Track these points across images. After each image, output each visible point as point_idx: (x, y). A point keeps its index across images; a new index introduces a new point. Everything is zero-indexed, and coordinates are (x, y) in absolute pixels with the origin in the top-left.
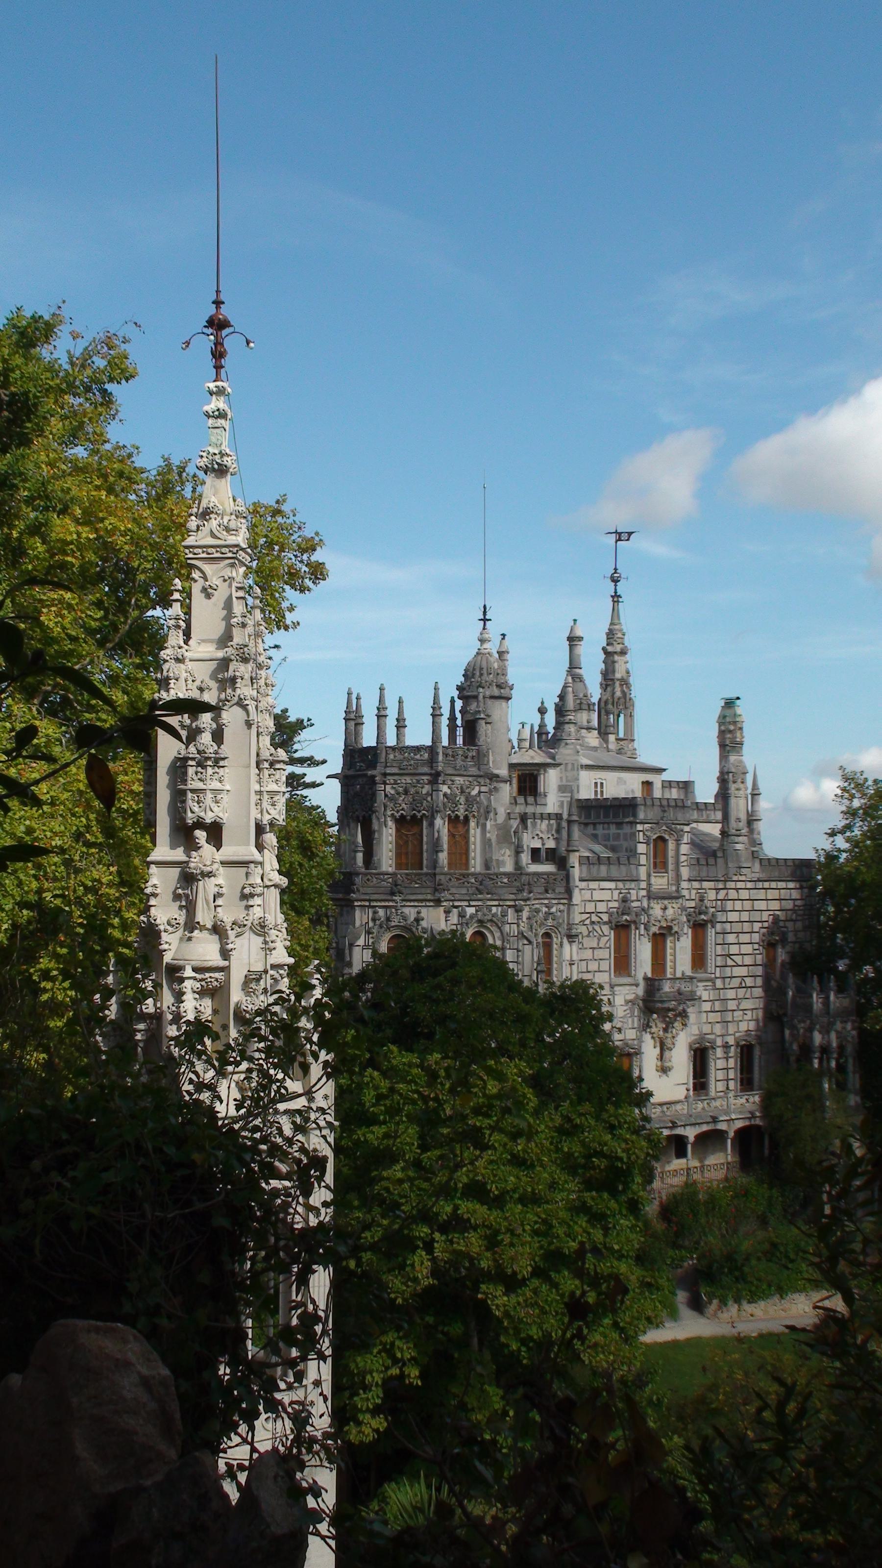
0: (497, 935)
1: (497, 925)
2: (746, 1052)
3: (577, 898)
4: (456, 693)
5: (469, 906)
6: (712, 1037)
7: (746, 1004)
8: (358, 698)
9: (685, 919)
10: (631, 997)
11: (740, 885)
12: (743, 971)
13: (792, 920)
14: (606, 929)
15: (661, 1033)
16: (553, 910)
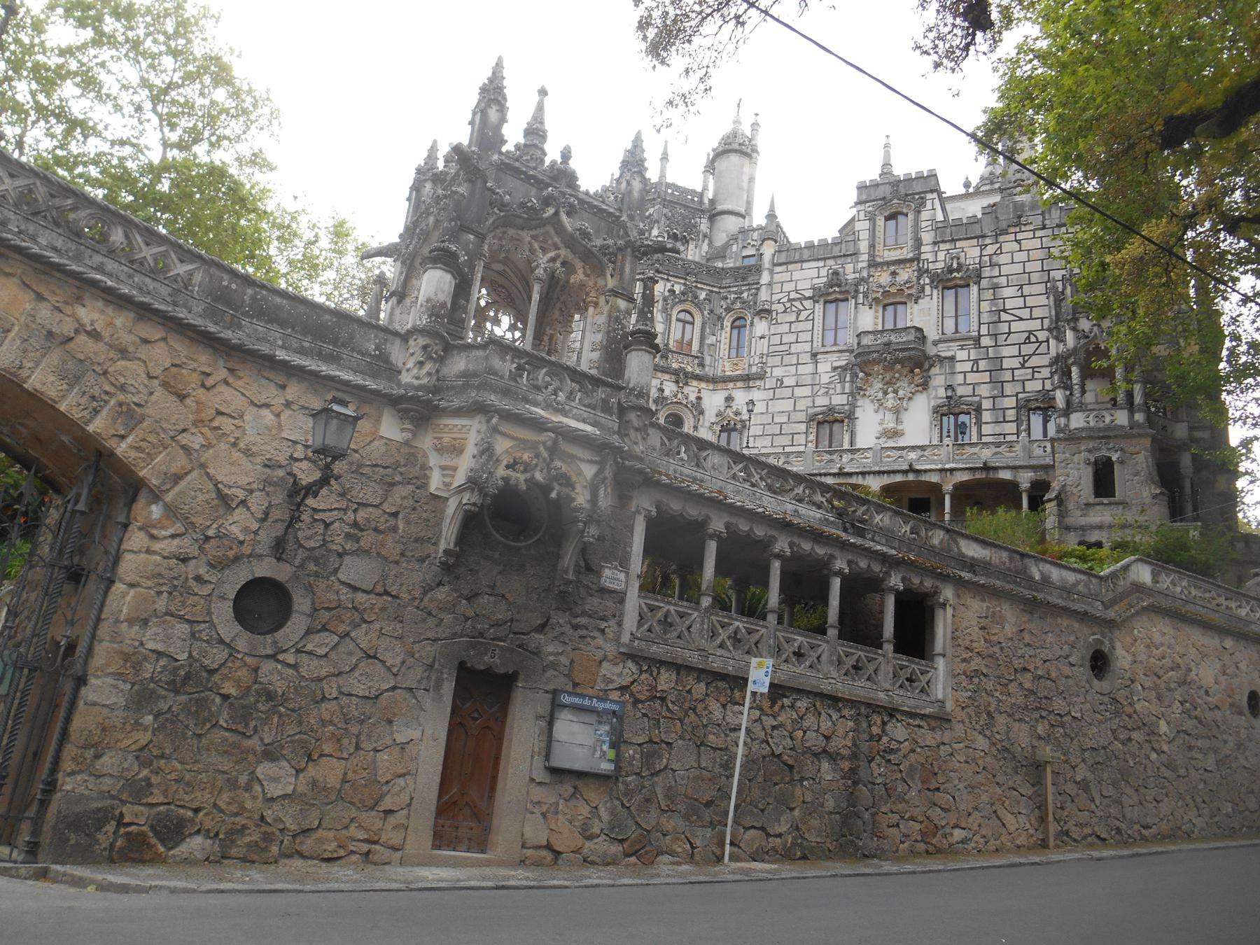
6: (977, 399)
9: (927, 281)
11: (1019, 236)
12: (1036, 325)
14: (808, 304)
15: (880, 395)
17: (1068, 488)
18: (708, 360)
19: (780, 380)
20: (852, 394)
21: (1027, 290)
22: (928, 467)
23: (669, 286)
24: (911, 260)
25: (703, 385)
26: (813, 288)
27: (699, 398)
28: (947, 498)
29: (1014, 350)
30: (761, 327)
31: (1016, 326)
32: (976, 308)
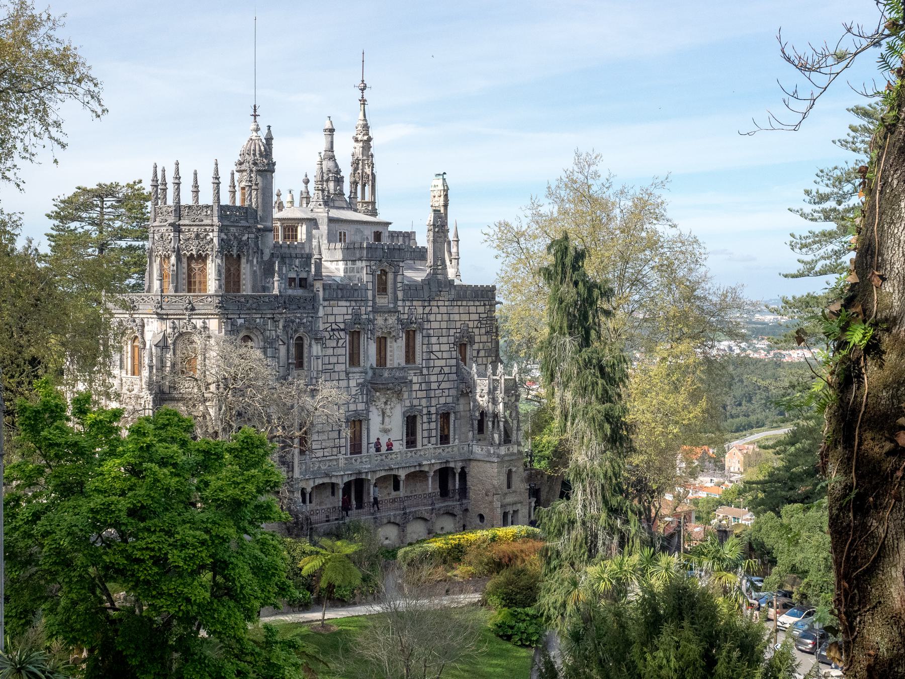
0: (261, 337)
2: (445, 417)
3: (321, 313)
4: (235, 168)
7: (443, 385)
8: (164, 171)
10: (361, 381)
14: (342, 334)
16: (305, 320)
20: (367, 403)
30: (316, 349)
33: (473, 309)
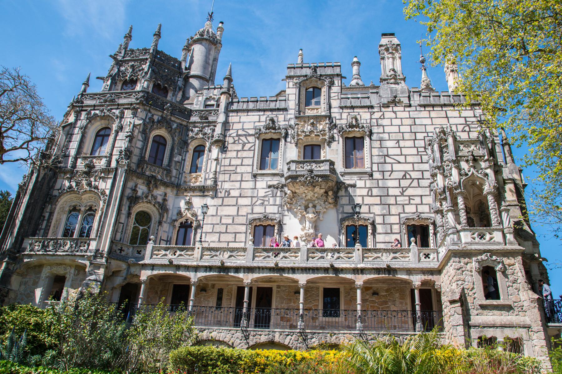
1: (112, 118)
5: (94, 110)
13: (463, 131)
14: (251, 139)
17: (466, 291)
18: (174, 172)
19: (228, 192)
20: (281, 206)
21: (402, 144)
22: (344, 266)
23: (150, 115)
24: (325, 117)
25: (169, 190)
26: (255, 128)
27: (165, 200)
28: (359, 292)
29: (395, 183)
31: (396, 167)
32: (368, 152)
33: (450, 114)
